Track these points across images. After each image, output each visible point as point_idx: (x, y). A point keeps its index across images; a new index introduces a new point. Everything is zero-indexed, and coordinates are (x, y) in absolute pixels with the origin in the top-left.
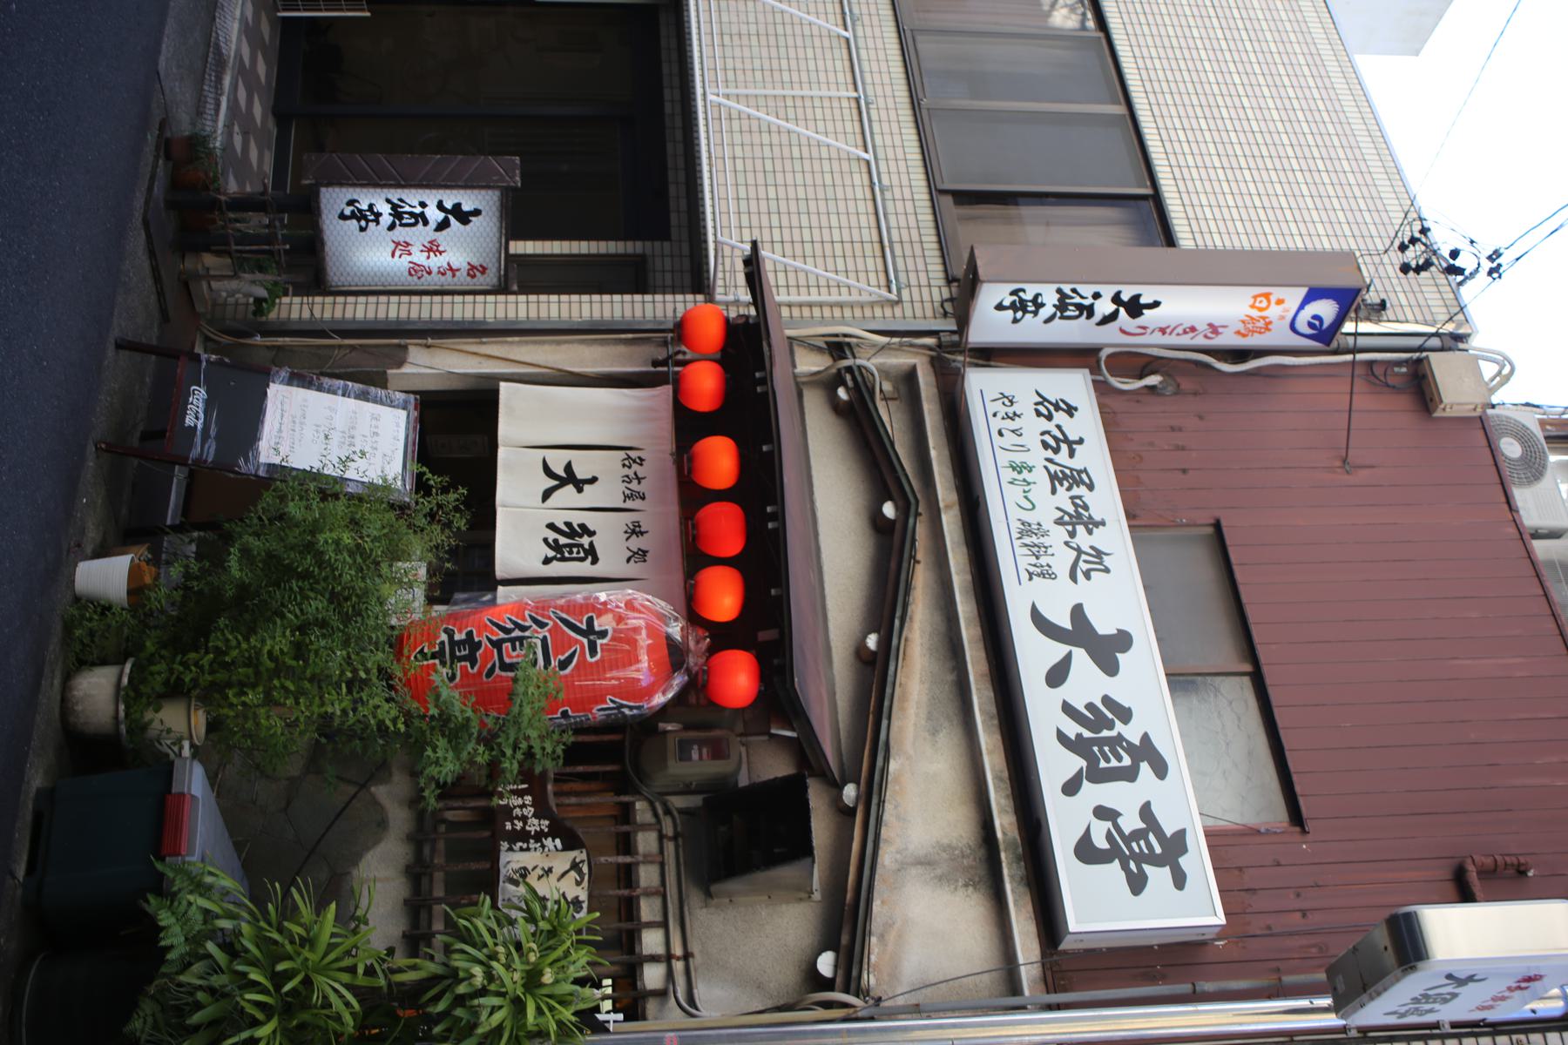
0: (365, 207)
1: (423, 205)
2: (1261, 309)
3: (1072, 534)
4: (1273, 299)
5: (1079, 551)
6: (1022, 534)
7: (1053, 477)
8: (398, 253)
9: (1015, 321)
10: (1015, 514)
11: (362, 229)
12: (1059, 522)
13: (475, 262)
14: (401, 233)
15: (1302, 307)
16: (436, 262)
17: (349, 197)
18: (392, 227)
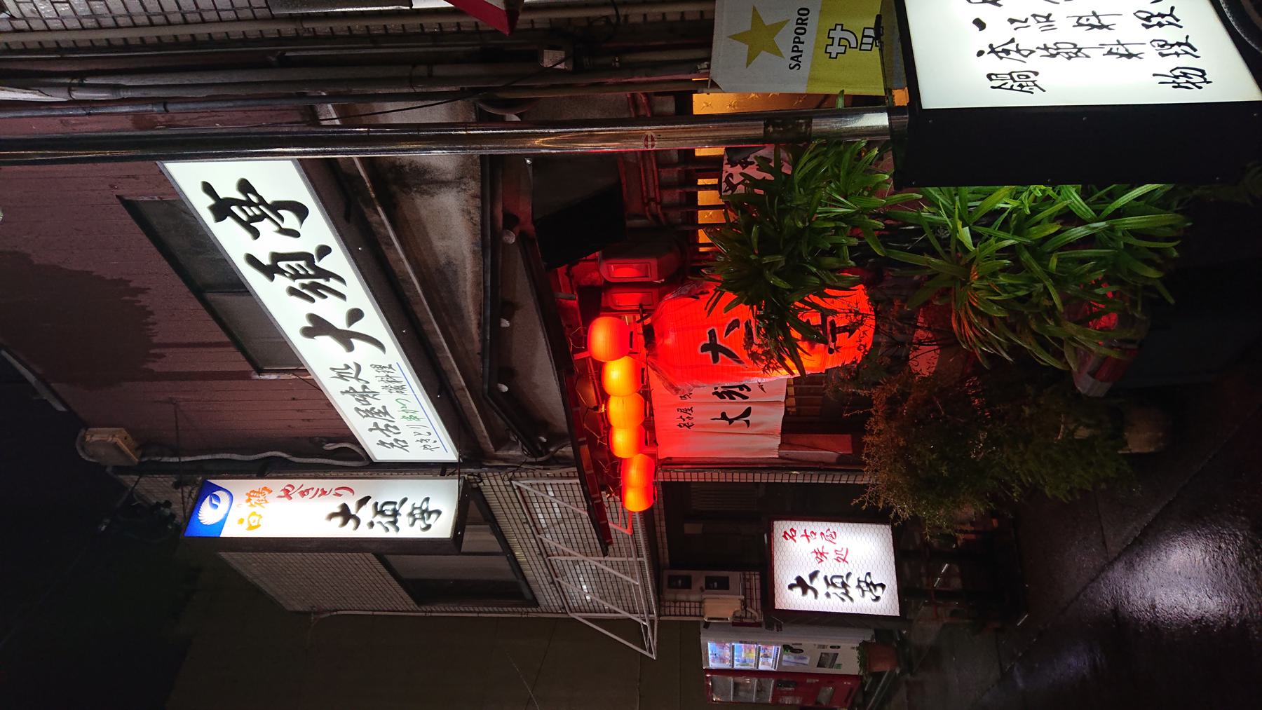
0: (868, 594)
1: (828, 595)
2: (254, 514)
3: (364, 387)
4: (246, 525)
5: (356, 378)
6: (402, 387)
7: (386, 413)
8: (844, 553)
9: (427, 499)
10: (410, 396)
11: (869, 574)
12: (376, 393)
13: (790, 540)
14: (842, 570)
15: (226, 515)
16: (817, 543)
17: (881, 601)
18: (849, 575)
